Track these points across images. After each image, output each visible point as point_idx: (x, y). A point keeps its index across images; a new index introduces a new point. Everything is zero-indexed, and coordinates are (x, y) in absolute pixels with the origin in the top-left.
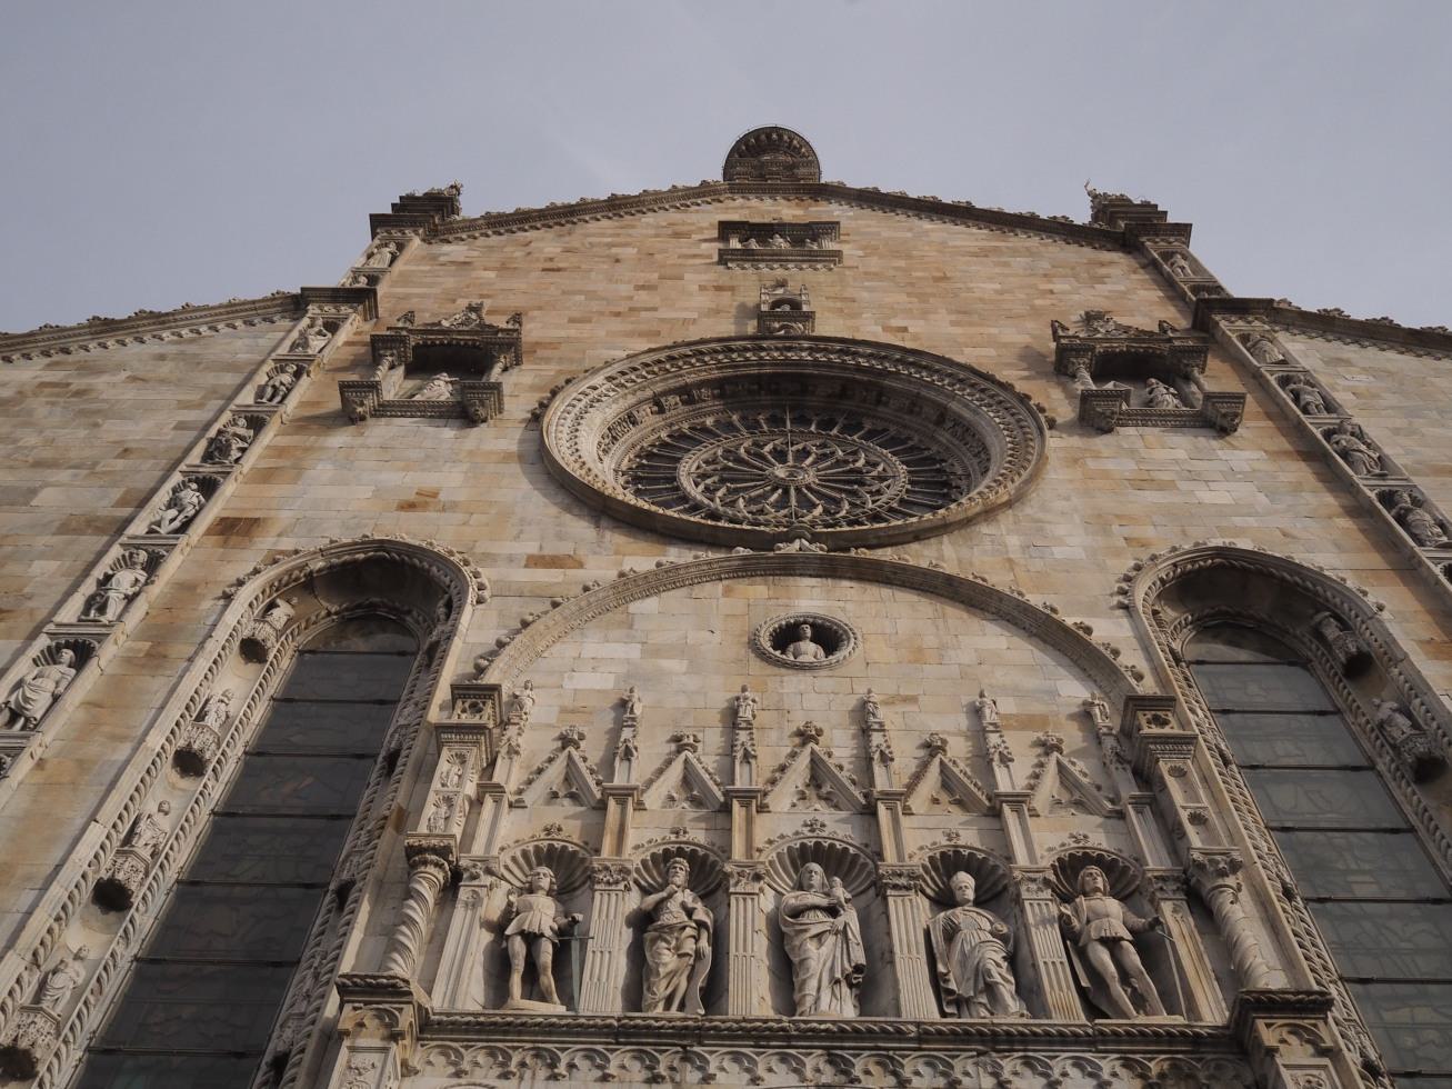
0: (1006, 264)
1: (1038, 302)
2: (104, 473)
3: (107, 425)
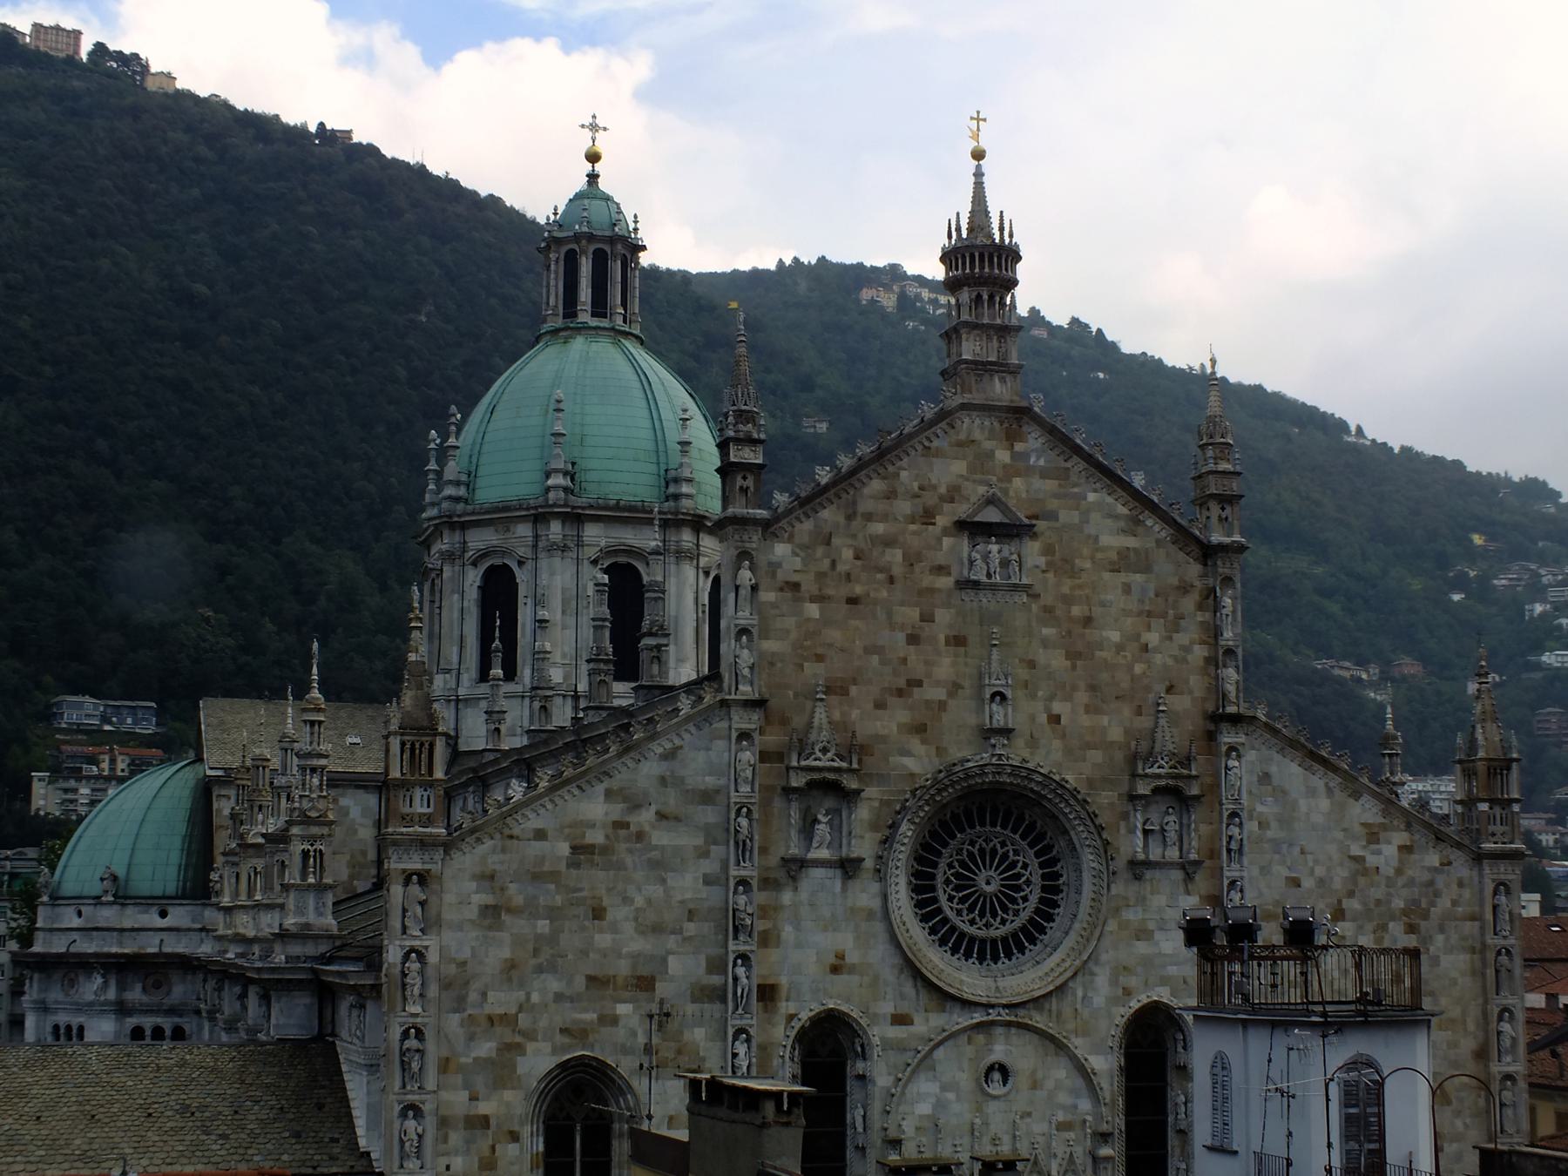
0: (1127, 589)
1: (1139, 669)
2: (690, 938)
3: (673, 881)
